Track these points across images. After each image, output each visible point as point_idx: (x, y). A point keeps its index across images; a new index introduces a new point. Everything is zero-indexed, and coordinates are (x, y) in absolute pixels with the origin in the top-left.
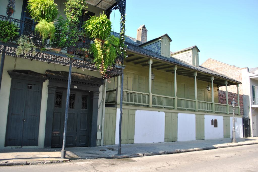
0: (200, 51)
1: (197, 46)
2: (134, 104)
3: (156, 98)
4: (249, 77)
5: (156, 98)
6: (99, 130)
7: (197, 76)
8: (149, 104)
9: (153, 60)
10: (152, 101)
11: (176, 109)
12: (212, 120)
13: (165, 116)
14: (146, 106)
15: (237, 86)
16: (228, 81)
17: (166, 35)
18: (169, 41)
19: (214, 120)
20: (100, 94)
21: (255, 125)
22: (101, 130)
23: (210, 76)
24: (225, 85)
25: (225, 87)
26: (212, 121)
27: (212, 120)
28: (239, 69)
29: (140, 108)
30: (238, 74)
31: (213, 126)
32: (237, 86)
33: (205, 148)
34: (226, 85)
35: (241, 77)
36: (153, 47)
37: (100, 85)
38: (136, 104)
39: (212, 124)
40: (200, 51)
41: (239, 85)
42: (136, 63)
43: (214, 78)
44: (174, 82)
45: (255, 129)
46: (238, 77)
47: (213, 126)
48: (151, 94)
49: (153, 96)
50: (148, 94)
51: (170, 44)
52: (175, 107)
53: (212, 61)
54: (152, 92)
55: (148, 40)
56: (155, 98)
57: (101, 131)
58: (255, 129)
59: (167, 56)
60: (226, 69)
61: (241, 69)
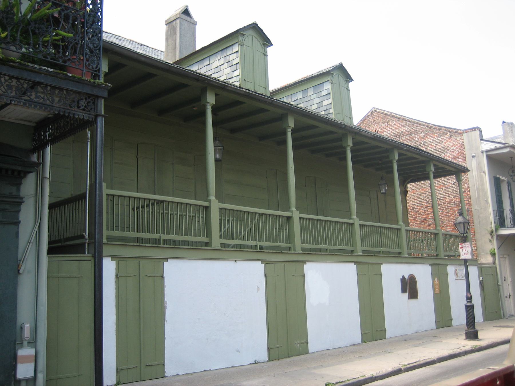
0: (352, 80)
1: (345, 65)
2: (159, 240)
3: (233, 220)
4: (485, 154)
5: (233, 220)
6: (25, 343)
7: (351, 147)
8: (211, 239)
9: (216, 95)
10: (221, 230)
11: (297, 251)
12: (403, 277)
13: (266, 276)
14: (201, 244)
15: (459, 180)
16: (435, 165)
17: (255, 27)
18: (264, 44)
19: (406, 277)
20: (23, 207)
21: (509, 283)
22: (33, 342)
23: (387, 151)
24: (426, 177)
25: (428, 182)
26: (403, 280)
27: (403, 277)
28: (456, 132)
29: (180, 253)
30: (456, 148)
31: (406, 295)
32: (459, 180)
33: (400, 366)
34: (432, 176)
35: (462, 154)
36: (215, 65)
37: (26, 173)
38: (164, 240)
39: (404, 291)
40: (352, 80)
41: (463, 176)
42: (162, 112)
43: (400, 155)
44: (285, 174)
45: (510, 296)
46: (455, 154)
47: (406, 295)
48: (215, 205)
49: (221, 209)
50: (206, 204)
51: (265, 55)
52: (294, 245)
53: (383, 115)
54: (216, 197)
55: (198, 48)
56: (228, 220)
57: (35, 347)
58: (510, 296)
59: (261, 91)
60: (422, 135)
61: (461, 131)
